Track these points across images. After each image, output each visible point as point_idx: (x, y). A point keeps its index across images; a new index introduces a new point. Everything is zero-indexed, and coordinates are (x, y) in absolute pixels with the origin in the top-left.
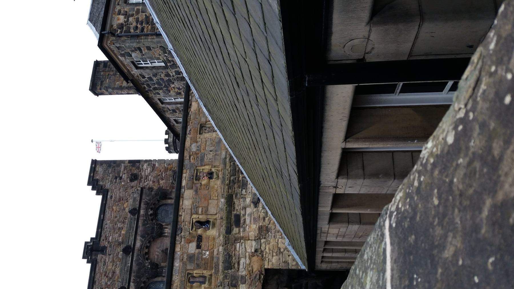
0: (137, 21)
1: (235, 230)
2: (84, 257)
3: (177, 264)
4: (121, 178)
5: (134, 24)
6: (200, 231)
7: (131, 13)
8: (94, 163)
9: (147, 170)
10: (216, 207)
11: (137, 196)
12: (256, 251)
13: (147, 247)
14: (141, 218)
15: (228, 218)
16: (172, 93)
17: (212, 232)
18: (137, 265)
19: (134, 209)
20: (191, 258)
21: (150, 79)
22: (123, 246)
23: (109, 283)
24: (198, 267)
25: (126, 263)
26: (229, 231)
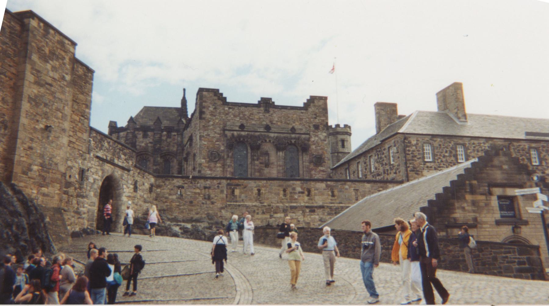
0: (413, 151)
1: (308, 210)
2: (262, 98)
4: (316, 118)
5: (411, 150)
6: (306, 193)
7: (418, 147)
8: (326, 98)
11: (304, 131)
12: (299, 221)
13: (270, 141)
14: (288, 135)
17: (306, 198)
18: (259, 136)
19: (295, 130)
21: (383, 154)
22: (269, 124)
24: (291, 193)
25: (259, 128)
26: (307, 207)
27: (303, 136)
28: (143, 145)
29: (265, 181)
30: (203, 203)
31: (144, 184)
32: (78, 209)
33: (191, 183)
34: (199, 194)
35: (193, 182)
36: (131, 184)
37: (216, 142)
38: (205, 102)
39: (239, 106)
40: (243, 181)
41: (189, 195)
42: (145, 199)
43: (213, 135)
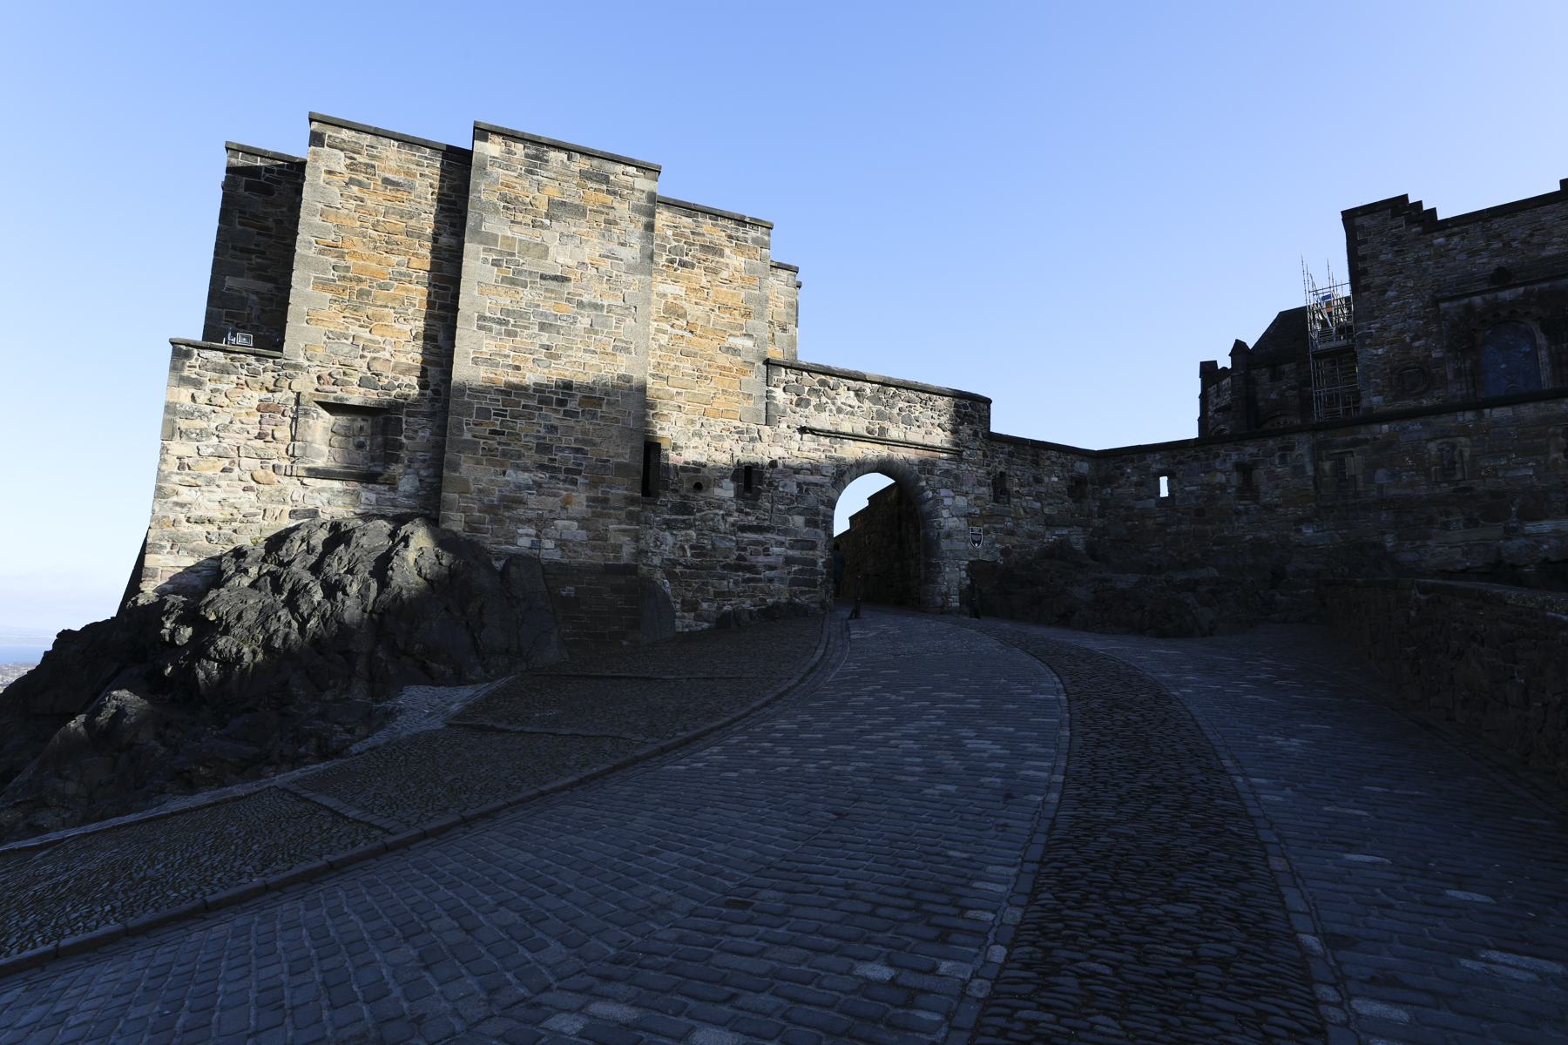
23: (1515, 244)
28: (1273, 396)
29: (1469, 415)
30: (1238, 513)
31: (1038, 480)
32: (740, 558)
33: (1196, 458)
34: (1223, 487)
35: (1202, 455)
36: (980, 484)
37: (1413, 340)
38: (1365, 242)
39: (1486, 220)
40: (1376, 428)
41: (1192, 492)
42: (1049, 517)
43: (1400, 326)
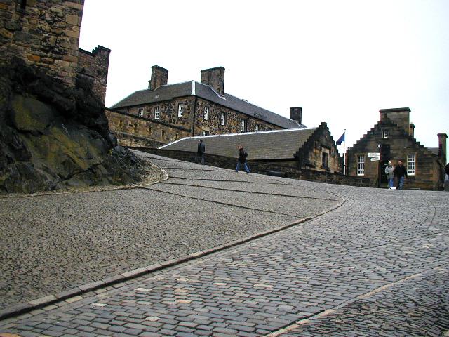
3: (126, 116)
9: (102, 81)
10: (141, 134)
11: (91, 73)
15: (138, 138)
16: (162, 114)
17: (133, 130)
20: (127, 122)
26: (134, 137)
27: (90, 78)
